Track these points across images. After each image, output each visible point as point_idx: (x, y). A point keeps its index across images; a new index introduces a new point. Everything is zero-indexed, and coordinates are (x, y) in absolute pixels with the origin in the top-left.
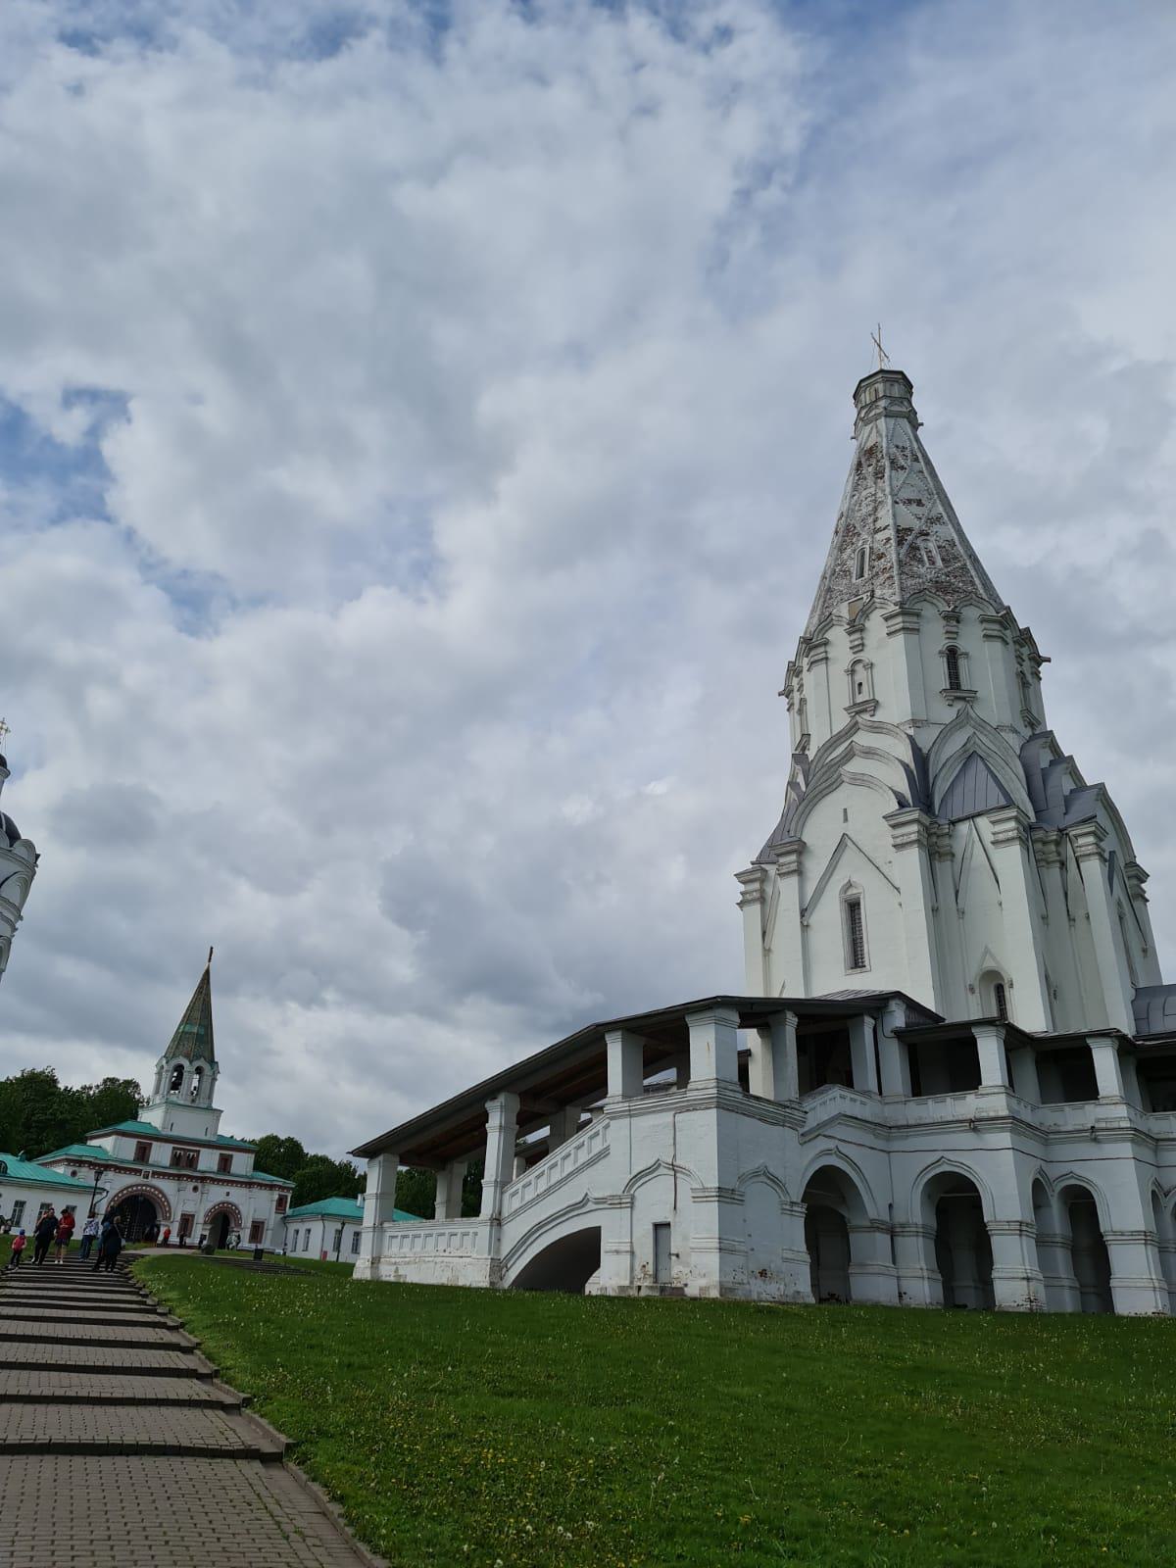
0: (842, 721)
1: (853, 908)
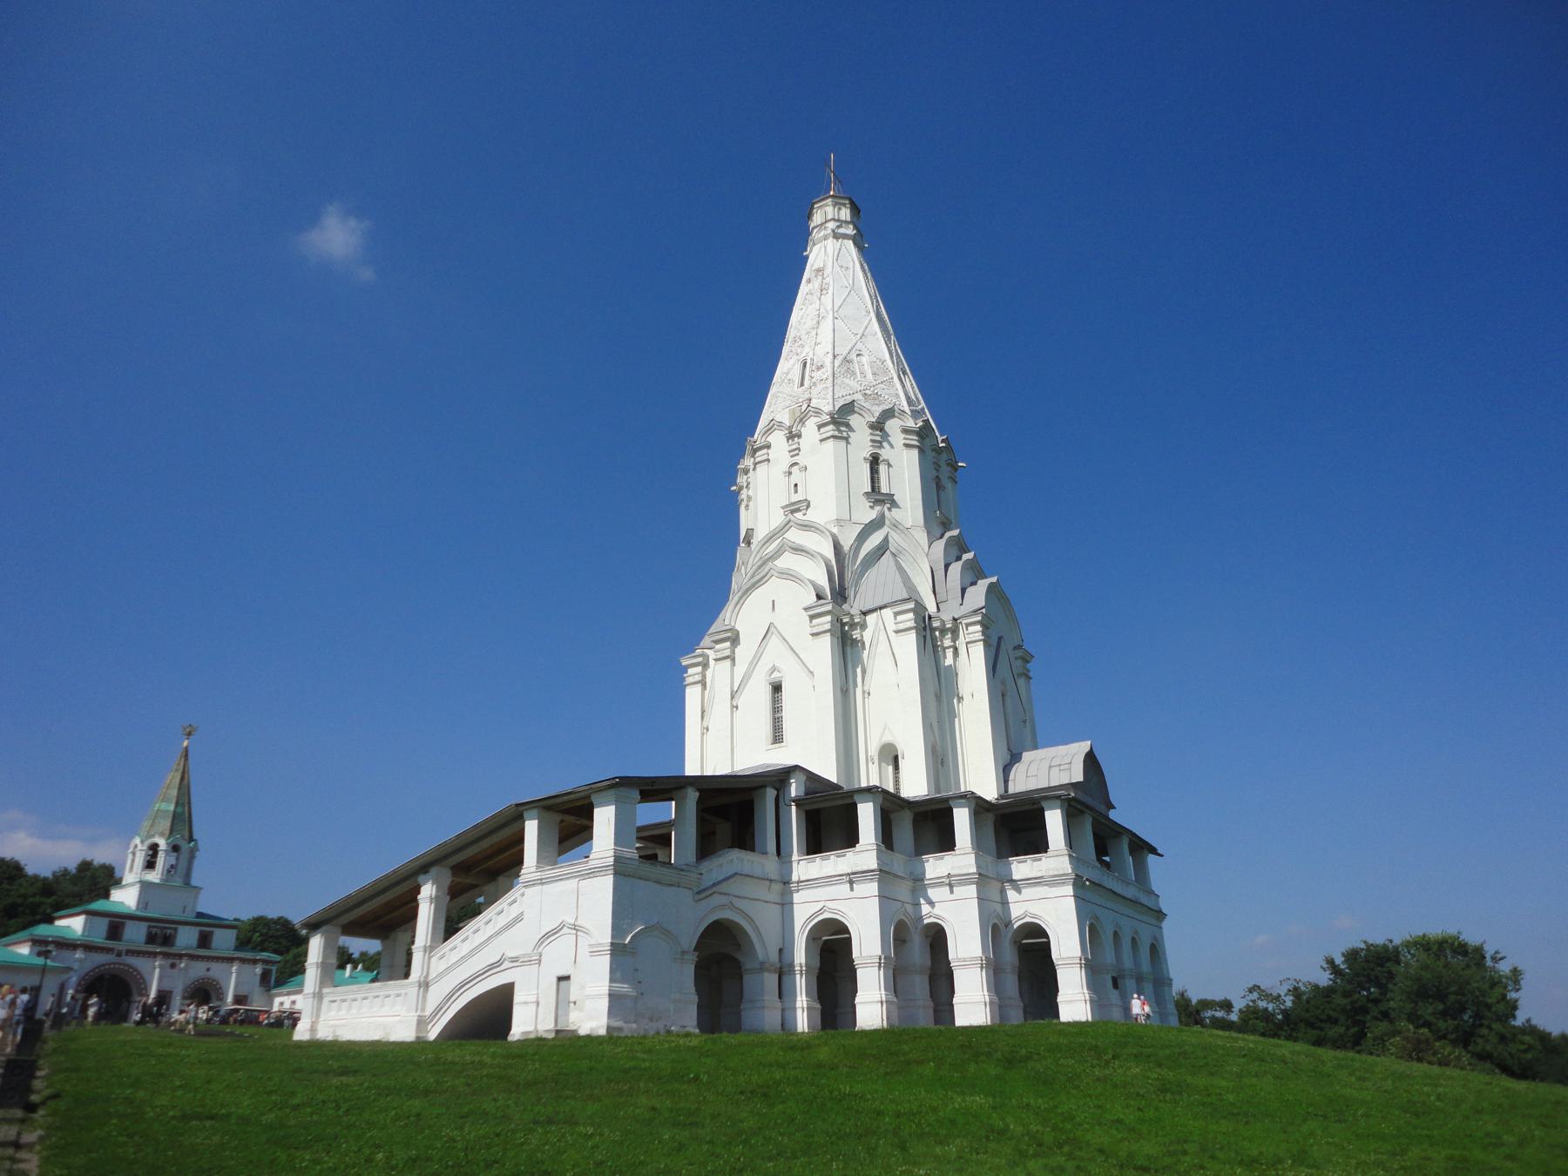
0: (778, 518)
1: (777, 688)
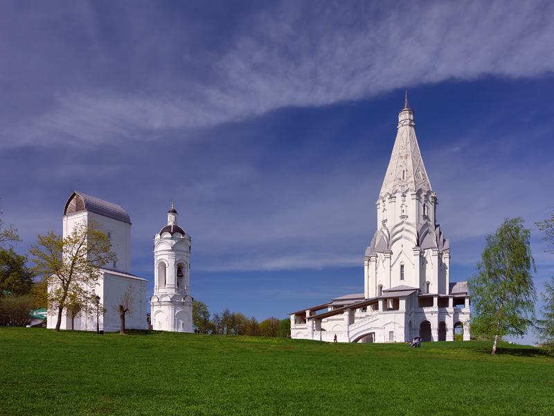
0: (400, 221)
1: (402, 266)
